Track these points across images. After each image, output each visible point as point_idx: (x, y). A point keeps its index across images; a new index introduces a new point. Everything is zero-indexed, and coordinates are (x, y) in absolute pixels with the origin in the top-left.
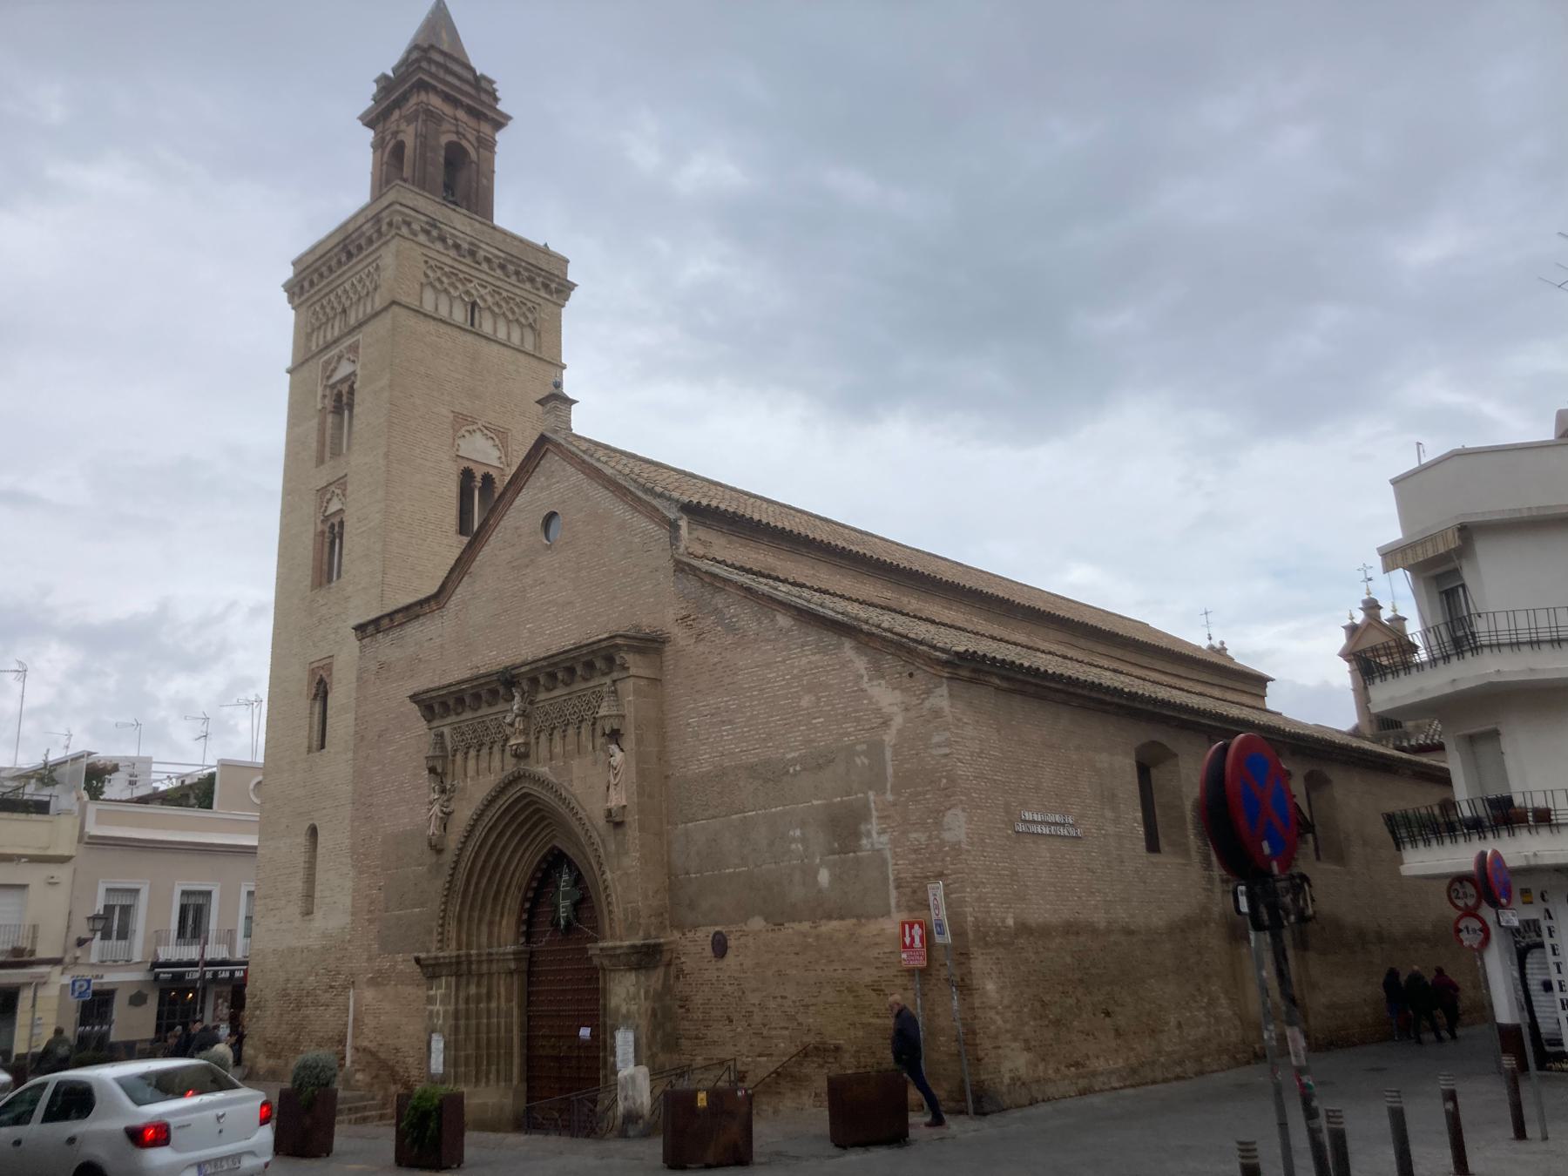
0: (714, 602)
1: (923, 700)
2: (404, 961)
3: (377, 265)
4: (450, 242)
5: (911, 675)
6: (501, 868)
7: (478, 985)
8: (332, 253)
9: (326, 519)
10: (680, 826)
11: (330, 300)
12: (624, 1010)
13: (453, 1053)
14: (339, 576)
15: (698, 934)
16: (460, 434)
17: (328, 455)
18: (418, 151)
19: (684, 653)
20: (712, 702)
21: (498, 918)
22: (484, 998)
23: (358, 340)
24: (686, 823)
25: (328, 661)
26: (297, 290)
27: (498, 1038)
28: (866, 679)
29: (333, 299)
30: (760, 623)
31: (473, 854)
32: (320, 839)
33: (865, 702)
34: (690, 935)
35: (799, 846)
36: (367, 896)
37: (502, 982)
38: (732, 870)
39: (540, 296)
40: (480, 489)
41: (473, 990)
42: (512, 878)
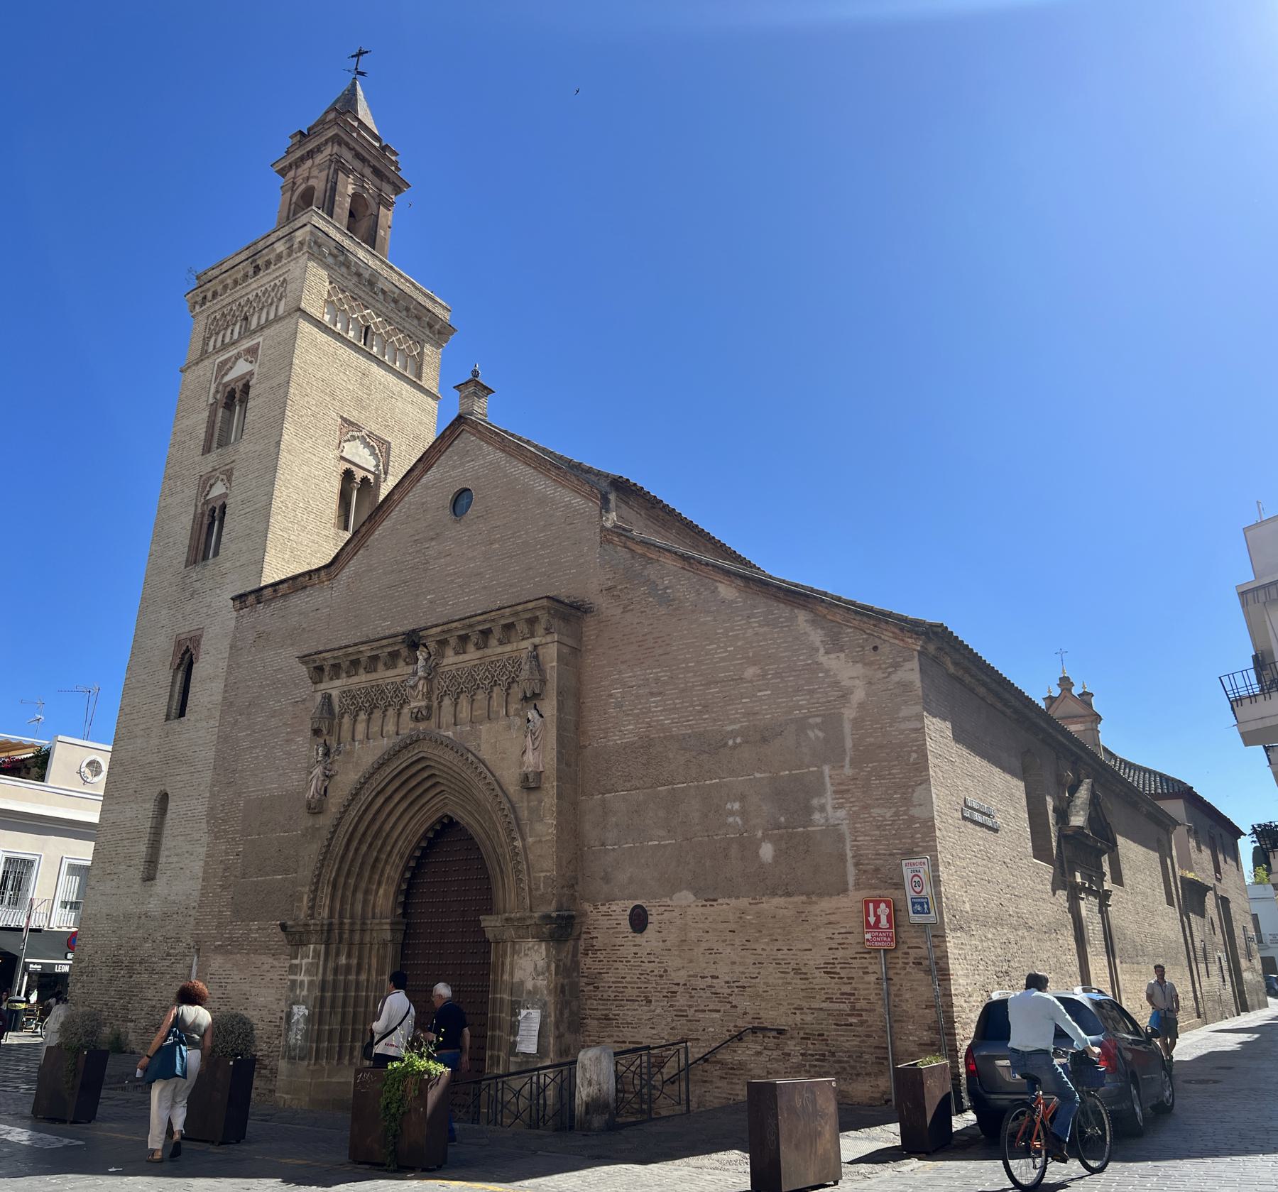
0: (646, 573)
1: (890, 673)
2: (259, 929)
3: (285, 279)
4: (354, 269)
5: (875, 648)
6: (384, 834)
7: (349, 956)
8: (240, 266)
9: (207, 502)
11: (231, 310)
12: (529, 985)
13: (316, 1027)
14: (216, 554)
15: (614, 908)
16: (346, 438)
17: (215, 445)
18: (328, 194)
19: (610, 623)
20: (638, 673)
21: (374, 887)
22: (354, 970)
23: (258, 344)
25: (198, 633)
26: (199, 299)
27: (365, 1013)
28: (822, 651)
29: (234, 308)
30: (699, 593)
31: (357, 818)
32: (171, 805)
33: (820, 675)
34: (604, 909)
35: (738, 819)
36: (221, 861)
37: (374, 952)
38: (657, 843)
39: (424, 334)
40: (358, 490)
41: (343, 960)
42: (393, 847)
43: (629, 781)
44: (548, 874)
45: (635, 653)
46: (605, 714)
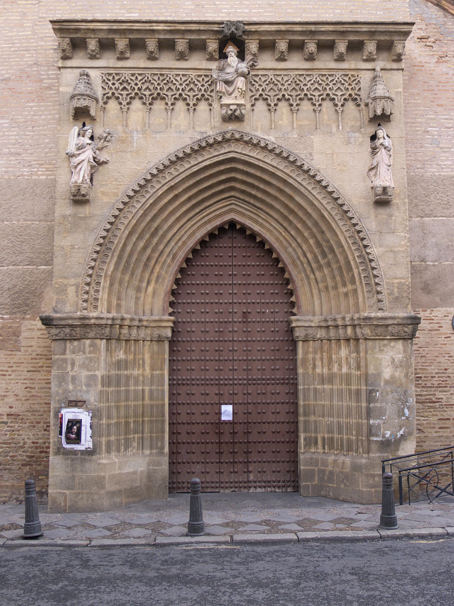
10: (413, 219)
19: (423, 68)
21: (144, 284)
24: (422, 217)
43: (448, 209)
44: (403, 281)
45: (451, 100)
46: (422, 147)
